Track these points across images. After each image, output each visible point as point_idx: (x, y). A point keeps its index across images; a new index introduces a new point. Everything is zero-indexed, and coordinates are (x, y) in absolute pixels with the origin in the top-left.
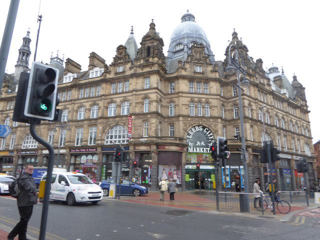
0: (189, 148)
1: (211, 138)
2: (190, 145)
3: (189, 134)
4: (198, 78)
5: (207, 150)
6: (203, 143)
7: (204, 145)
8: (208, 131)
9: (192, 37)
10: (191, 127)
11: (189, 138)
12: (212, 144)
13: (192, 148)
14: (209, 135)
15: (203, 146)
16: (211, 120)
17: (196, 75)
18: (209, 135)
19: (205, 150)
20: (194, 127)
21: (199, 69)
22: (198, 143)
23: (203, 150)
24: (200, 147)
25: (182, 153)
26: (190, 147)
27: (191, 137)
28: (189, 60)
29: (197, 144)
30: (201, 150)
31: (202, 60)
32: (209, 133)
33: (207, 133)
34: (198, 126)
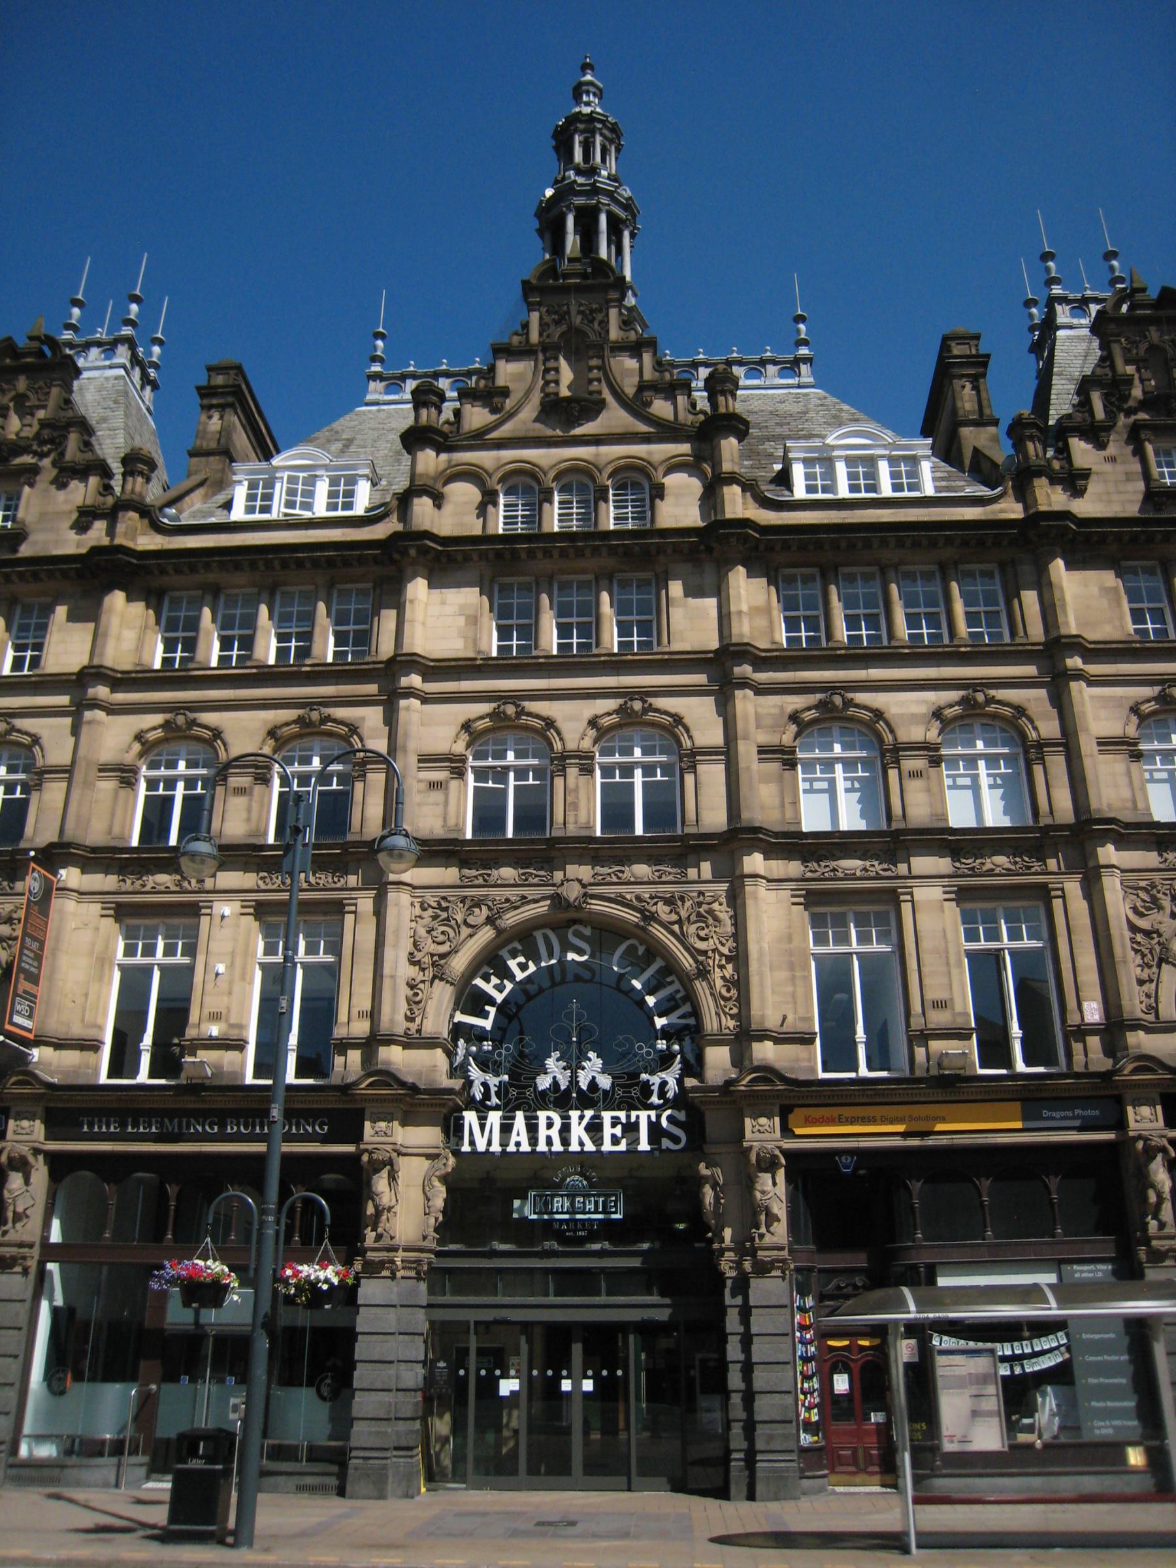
0: (470, 1117)
2: (477, 1092)
7: (605, 1082)
11: (478, 1036)
13: (494, 1118)
15: (590, 1098)
19: (608, 1131)
22: (554, 1071)
23: (594, 1129)
24: (561, 1099)
26: (482, 1109)
27: (487, 1024)
29: (544, 1083)
30: (578, 1131)
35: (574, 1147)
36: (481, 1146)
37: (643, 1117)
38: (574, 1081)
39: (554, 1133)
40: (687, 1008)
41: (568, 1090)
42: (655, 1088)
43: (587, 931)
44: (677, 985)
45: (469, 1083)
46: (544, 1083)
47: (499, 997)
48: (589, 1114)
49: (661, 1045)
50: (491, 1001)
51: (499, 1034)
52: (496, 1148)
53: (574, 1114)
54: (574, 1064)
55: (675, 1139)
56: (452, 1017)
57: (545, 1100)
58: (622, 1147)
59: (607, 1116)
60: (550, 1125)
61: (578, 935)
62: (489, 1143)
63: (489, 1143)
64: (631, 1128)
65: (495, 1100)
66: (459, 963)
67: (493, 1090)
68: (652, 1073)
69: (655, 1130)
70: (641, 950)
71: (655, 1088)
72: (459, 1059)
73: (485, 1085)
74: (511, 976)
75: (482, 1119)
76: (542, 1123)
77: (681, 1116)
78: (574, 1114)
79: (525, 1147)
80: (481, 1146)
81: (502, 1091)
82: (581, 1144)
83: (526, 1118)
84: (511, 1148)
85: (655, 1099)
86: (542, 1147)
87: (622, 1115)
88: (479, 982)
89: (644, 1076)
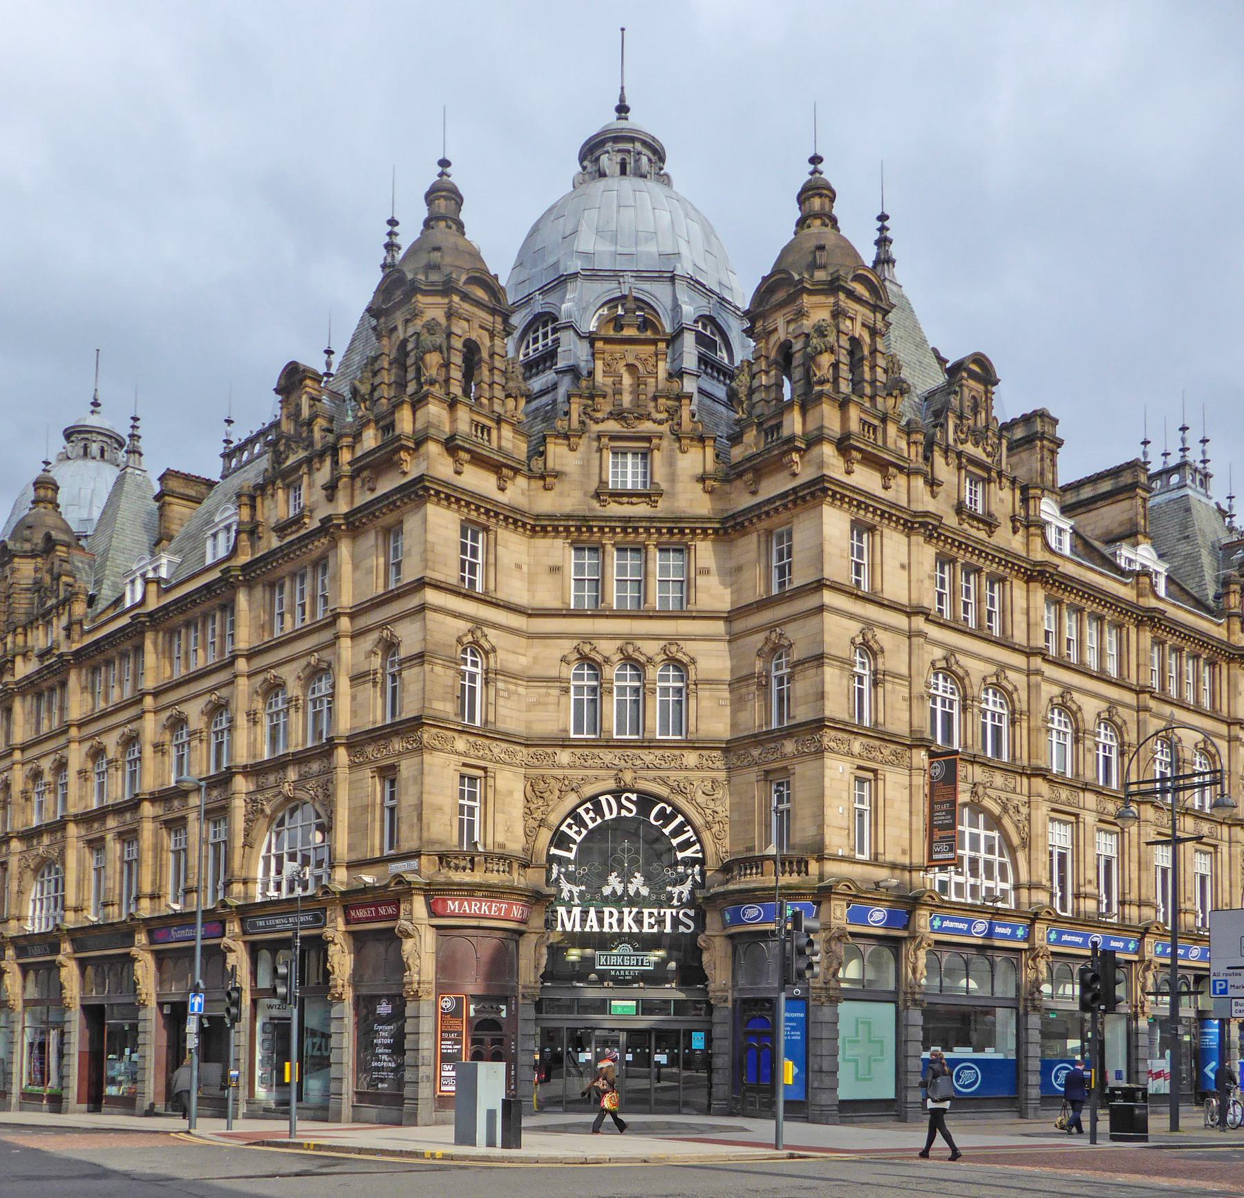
0: (561, 910)
1: (689, 853)
2: (565, 895)
3: (561, 840)
4: (628, 524)
5: (661, 921)
6: (637, 884)
7: (645, 891)
8: (665, 818)
9: (615, 275)
10: (571, 800)
12: (689, 882)
13: (577, 911)
14: (675, 842)
16: (691, 758)
17: (614, 509)
18: (675, 842)
19: (646, 920)
20: (594, 799)
21: (627, 474)
22: (614, 884)
23: (639, 921)
24: (617, 900)
25: (521, 933)
27: (572, 856)
28: (575, 424)
29: (607, 891)
30: (628, 920)
31: (649, 417)
32: (678, 831)
33: (667, 831)
34: (617, 794)
35: (626, 930)
36: (569, 928)
37: (668, 913)
38: (626, 889)
39: (614, 921)
40: (697, 847)
41: (622, 896)
42: (676, 896)
43: (634, 797)
44: (691, 833)
45: (561, 891)
46: (607, 891)
47: (578, 839)
48: (635, 910)
49: (681, 869)
50: (574, 842)
51: (579, 861)
52: (578, 929)
53: (626, 910)
54: (626, 878)
55: (688, 927)
56: (548, 850)
57: (606, 901)
58: (655, 930)
59: (646, 911)
60: (611, 914)
61: (628, 799)
62: (574, 926)
63: (574, 926)
64: (661, 921)
65: (577, 901)
66: (554, 819)
67: (576, 895)
68: (674, 886)
69: (676, 921)
70: (669, 809)
71: (676, 896)
72: (554, 876)
73: (570, 892)
74: (586, 826)
75: (569, 912)
76: (606, 915)
77: (692, 913)
78: (626, 910)
79: (596, 929)
80: (569, 928)
81: (581, 893)
82: (630, 927)
83: (597, 912)
84: (587, 929)
85: (675, 902)
86: (606, 929)
87: (655, 911)
88: (564, 828)
89: (669, 888)
